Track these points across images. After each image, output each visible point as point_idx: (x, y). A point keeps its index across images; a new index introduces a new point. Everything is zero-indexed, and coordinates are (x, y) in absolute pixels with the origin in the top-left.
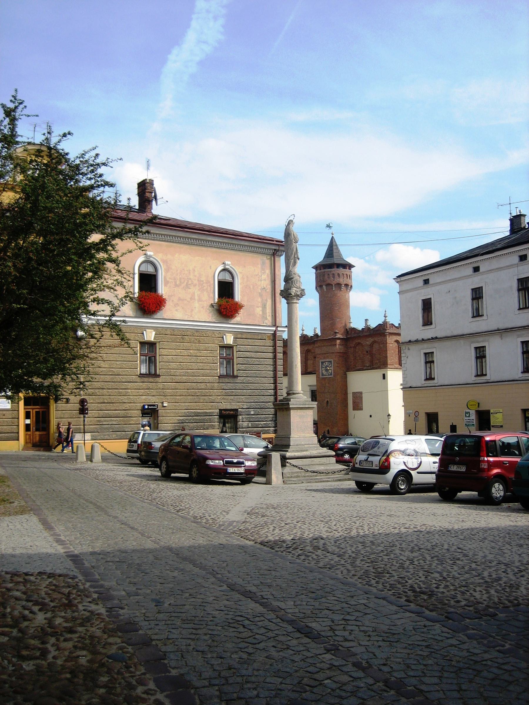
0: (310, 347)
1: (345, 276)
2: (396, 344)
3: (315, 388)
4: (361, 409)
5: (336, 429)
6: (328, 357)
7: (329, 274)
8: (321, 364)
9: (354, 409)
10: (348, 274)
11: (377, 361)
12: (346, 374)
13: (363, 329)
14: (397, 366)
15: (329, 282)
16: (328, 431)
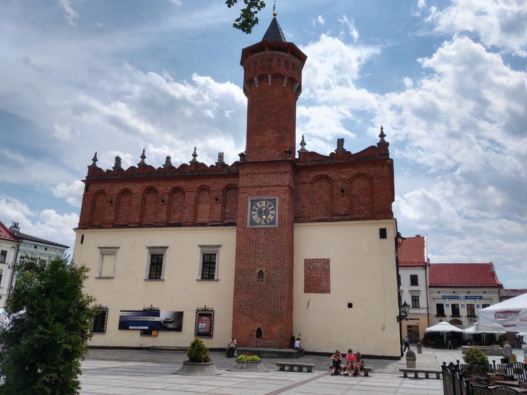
4: (327, 290)
5: (280, 326)
6: (267, 193)
8: (249, 204)
9: (308, 289)
11: (363, 208)
12: (293, 227)
16: (259, 331)
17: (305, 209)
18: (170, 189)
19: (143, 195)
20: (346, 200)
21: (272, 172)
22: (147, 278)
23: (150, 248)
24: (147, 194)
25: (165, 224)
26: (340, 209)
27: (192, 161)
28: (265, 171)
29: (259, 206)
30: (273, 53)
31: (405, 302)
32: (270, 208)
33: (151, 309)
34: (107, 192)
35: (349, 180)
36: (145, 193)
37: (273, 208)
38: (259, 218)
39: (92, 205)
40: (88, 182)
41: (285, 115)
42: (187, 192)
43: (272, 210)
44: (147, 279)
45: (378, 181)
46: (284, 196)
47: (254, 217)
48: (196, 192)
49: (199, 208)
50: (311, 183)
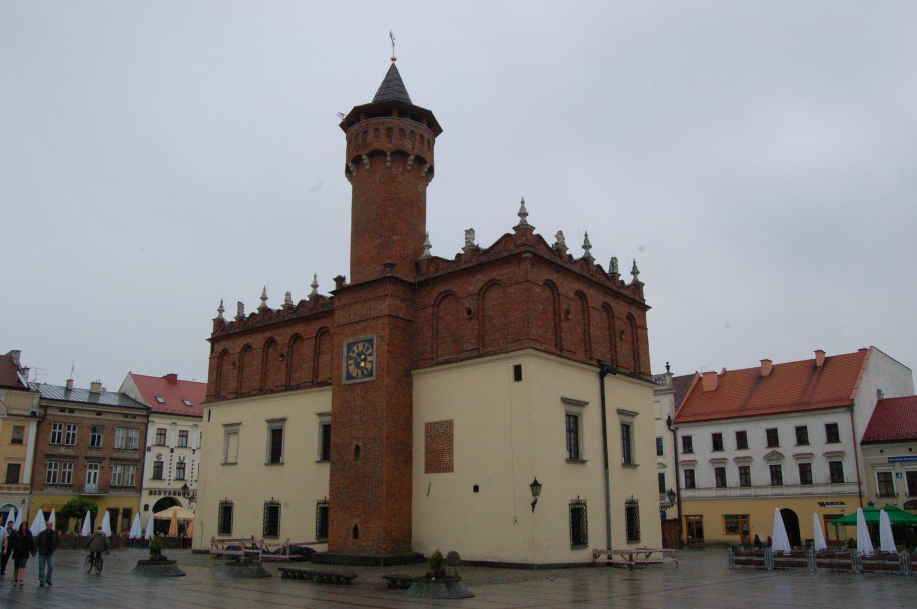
0: (326, 323)
1: (418, 137)
2: (548, 292)
3: (328, 420)
4: (449, 468)
7: (377, 130)
8: (345, 349)
10: (425, 135)
11: (498, 335)
13: (459, 255)
14: (552, 349)
15: (377, 145)
16: (356, 528)
17: (427, 346)
18: (289, 339)
19: (263, 351)
20: (474, 326)
21: (369, 299)
22: (319, 460)
23: (270, 421)
24: (268, 347)
25: (283, 388)
26: (466, 341)
27: (310, 295)
28: (362, 299)
29: (356, 351)
30: (368, 122)
31: (535, 480)
32: (368, 353)
33: (272, 502)
34: (231, 351)
35: (478, 294)
36: (266, 347)
37: (371, 352)
38: (356, 370)
39: (217, 370)
40: (213, 340)
41: (389, 209)
42: (307, 339)
43: (371, 354)
44: (266, 462)
45: (512, 290)
46: (382, 333)
47: (352, 368)
48: (316, 337)
49: (321, 360)
50: (433, 306)
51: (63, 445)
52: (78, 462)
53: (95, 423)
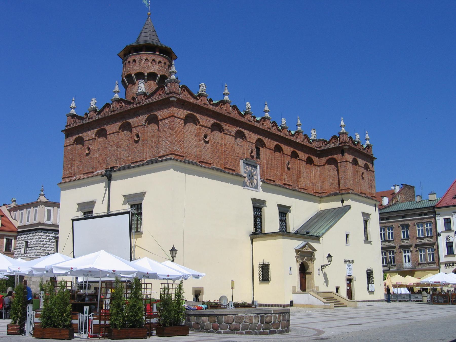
51: (387, 241)
52: (396, 250)
53: (403, 223)
